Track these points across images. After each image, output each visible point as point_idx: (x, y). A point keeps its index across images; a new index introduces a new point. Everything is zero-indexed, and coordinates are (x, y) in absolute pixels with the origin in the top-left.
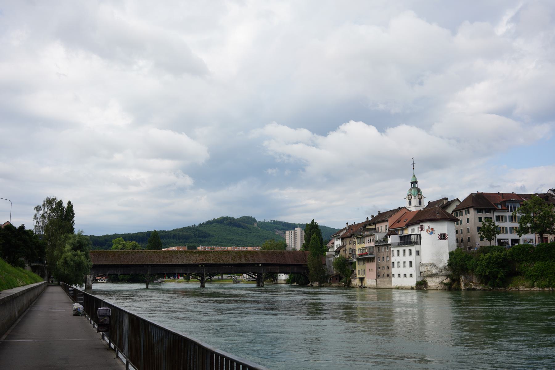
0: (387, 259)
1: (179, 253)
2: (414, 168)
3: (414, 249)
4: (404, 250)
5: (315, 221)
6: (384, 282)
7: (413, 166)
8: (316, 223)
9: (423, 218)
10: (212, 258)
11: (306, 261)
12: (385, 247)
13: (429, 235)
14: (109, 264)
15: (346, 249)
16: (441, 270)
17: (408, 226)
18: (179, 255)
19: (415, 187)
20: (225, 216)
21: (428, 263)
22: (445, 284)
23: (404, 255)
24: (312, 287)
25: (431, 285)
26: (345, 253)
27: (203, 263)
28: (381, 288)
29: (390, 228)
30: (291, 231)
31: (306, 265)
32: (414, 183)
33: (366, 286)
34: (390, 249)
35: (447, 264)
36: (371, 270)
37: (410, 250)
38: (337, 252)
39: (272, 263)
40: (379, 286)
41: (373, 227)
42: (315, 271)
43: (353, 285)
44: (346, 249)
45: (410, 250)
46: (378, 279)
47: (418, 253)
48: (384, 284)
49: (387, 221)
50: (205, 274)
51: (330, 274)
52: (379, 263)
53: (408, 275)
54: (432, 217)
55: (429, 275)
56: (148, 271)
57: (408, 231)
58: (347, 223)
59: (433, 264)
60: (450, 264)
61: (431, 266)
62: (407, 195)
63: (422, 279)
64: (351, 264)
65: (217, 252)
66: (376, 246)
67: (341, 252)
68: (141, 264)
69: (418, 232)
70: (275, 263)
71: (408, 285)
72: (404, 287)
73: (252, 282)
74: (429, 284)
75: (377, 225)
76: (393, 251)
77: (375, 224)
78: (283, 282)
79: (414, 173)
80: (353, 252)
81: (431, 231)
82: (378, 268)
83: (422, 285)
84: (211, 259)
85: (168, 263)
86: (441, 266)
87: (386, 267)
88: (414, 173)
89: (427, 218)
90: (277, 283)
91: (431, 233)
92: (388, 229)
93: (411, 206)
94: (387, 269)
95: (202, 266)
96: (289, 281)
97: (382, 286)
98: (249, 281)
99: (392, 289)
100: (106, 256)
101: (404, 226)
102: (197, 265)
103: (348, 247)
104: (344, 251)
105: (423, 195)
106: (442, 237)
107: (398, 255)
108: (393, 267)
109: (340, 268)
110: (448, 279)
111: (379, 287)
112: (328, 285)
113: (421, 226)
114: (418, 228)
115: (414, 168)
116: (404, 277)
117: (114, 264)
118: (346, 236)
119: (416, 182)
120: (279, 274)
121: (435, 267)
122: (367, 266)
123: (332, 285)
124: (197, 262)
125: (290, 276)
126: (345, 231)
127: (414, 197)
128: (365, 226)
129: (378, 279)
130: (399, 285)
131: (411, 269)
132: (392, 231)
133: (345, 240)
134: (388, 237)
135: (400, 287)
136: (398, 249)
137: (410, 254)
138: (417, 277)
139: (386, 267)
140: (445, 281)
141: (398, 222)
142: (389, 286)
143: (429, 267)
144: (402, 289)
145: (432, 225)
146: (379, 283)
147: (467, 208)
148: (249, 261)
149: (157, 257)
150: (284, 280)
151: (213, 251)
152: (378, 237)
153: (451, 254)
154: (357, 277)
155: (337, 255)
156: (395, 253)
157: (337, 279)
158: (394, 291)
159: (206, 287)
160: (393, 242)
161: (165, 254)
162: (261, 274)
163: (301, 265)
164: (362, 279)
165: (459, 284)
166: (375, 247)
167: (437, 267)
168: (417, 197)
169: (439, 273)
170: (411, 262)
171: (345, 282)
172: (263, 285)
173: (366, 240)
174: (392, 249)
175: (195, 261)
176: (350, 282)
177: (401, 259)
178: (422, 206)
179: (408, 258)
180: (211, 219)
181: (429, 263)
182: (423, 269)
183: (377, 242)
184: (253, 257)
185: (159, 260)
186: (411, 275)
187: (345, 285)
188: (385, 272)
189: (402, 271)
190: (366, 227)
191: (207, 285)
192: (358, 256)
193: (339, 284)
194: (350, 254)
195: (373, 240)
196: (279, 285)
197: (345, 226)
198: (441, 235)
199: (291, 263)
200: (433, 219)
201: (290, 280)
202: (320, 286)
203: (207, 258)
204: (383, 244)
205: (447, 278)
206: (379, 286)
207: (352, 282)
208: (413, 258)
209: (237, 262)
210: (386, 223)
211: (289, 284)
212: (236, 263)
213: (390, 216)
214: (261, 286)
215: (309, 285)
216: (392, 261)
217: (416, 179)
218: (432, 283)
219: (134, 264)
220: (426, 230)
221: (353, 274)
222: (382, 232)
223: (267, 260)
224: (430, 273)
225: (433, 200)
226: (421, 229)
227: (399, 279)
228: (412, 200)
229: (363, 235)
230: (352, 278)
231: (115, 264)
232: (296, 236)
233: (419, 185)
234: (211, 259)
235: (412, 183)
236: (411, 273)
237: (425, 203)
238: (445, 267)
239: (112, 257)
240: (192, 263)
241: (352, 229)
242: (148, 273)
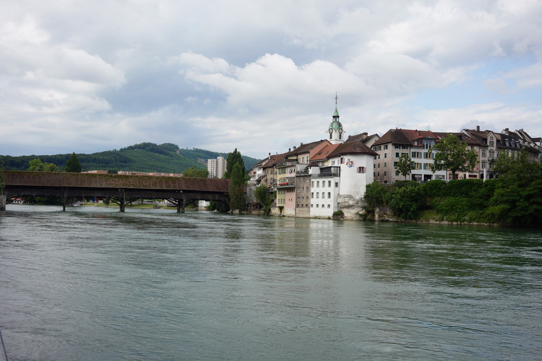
0: (306, 190)
1: (97, 177)
3: (333, 180)
4: (324, 182)
5: (238, 151)
6: (303, 211)
8: (238, 152)
9: (344, 151)
10: (133, 182)
11: (227, 189)
12: (306, 178)
13: (348, 168)
14: (24, 185)
15: (267, 179)
16: (358, 202)
17: (329, 158)
18: (98, 179)
19: (336, 121)
20: (147, 142)
21: (346, 194)
22: (361, 215)
23: (324, 186)
24: (232, 214)
25: (348, 215)
26: (267, 182)
27: (123, 187)
28: (300, 217)
29: (311, 160)
30: (213, 160)
31: (228, 192)
32: (336, 117)
33: (285, 214)
34: (310, 180)
35: (363, 196)
36: (291, 200)
37: (330, 182)
38: (259, 181)
39: (194, 190)
40: (298, 215)
41: (295, 158)
42: (236, 199)
43: (273, 213)
44: (268, 178)
45: (330, 182)
46: (297, 209)
47: (337, 185)
48: (302, 213)
49: (309, 153)
50: (124, 199)
51: (251, 202)
53: (326, 206)
54: (353, 151)
55: (346, 206)
56: (65, 194)
57: (329, 164)
58: (270, 154)
59: (350, 196)
60: (367, 197)
61: (348, 197)
62: (328, 129)
63: (339, 209)
64: (272, 193)
65: (137, 177)
66: (297, 176)
67: (263, 181)
68: (57, 186)
69: (338, 164)
70: (197, 189)
71: (325, 215)
72: (322, 217)
73: (172, 208)
74: (346, 215)
75: (299, 157)
76: (313, 182)
77: (297, 155)
78: (204, 209)
80: (274, 182)
81: (350, 163)
82: (298, 197)
83: (339, 215)
84: (131, 184)
85: (86, 186)
86: (358, 198)
87: (305, 198)
89: (347, 152)
90: (197, 210)
91: (351, 166)
92: (310, 161)
93: (331, 140)
94: (306, 199)
95: (122, 190)
96: (210, 208)
98: (170, 206)
99: (310, 218)
100: (21, 177)
101: (325, 158)
102: (116, 190)
103: (269, 176)
104: (265, 180)
105: (343, 129)
106: (361, 170)
107: (318, 186)
108: (313, 197)
109: (261, 197)
110: (364, 210)
111: (297, 216)
112: (248, 213)
113: (342, 159)
114: (339, 160)
116: (322, 207)
117: (28, 185)
118: (268, 166)
119: (338, 117)
120: (200, 201)
121: (352, 199)
122: (287, 196)
123: (252, 213)
124: (117, 186)
125: (211, 203)
126: (267, 161)
127: (335, 131)
128: (287, 156)
129: (297, 209)
130: (317, 215)
131: (329, 199)
132: (313, 163)
133: (266, 170)
134: (309, 168)
135: (318, 216)
136: (318, 180)
137: (330, 185)
138: (335, 207)
139: (305, 198)
140: (360, 213)
141: (320, 154)
142: (307, 216)
143: (346, 199)
144: (319, 218)
145: (352, 158)
146: (298, 212)
147: (386, 143)
148: (170, 187)
149: (75, 180)
150: (205, 207)
151: (134, 176)
152: (299, 168)
153: (368, 187)
154: (277, 206)
155: (258, 184)
156: (315, 184)
157: (257, 208)
158: (311, 220)
159: (126, 211)
160: (314, 173)
161: (83, 177)
162: (182, 200)
163: (223, 193)
164: (281, 208)
165: (374, 215)
166: (296, 178)
167: (354, 199)
168: (338, 130)
169: (355, 204)
170: (329, 193)
171: (265, 211)
172: (183, 211)
173: (288, 170)
174: (312, 180)
175: (114, 186)
176: (270, 210)
177: (321, 190)
178: (342, 140)
179: (327, 189)
180: (133, 144)
181: (347, 195)
182: (340, 200)
183: (298, 173)
184: (175, 183)
185: (77, 183)
186: (329, 206)
187: (265, 213)
188: (304, 202)
189: (321, 201)
190: (287, 158)
191: (127, 210)
192: (279, 186)
193: (259, 212)
194: (271, 183)
195: (294, 170)
196: (199, 212)
197: (268, 156)
198: (360, 168)
199: (212, 191)
200: (354, 153)
201: (211, 207)
202: (241, 214)
203: (127, 183)
204: (304, 175)
205: (363, 210)
207: (272, 211)
208: (332, 189)
209: (158, 188)
210: (308, 155)
211: (209, 211)
212: (157, 189)
213: (312, 148)
214: (182, 212)
215: (229, 212)
216: (312, 192)
217: (338, 113)
218: (348, 214)
219: (50, 186)
220: (345, 163)
221: (273, 203)
222: (303, 163)
223: (188, 187)
224: (347, 205)
225: (353, 134)
226: (341, 162)
227: (317, 209)
228: (333, 134)
229: (284, 166)
230: (272, 207)
231: (30, 185)
232: (218, 164)
233: (341, 120)
234: (131, 184)
235: (334, 117)
236: (329, 204)
237: (345, 138)
238: (362, 199)
239: (26, 178)
240: (111, 187)
241: (274, 160)
242: (65, 195)
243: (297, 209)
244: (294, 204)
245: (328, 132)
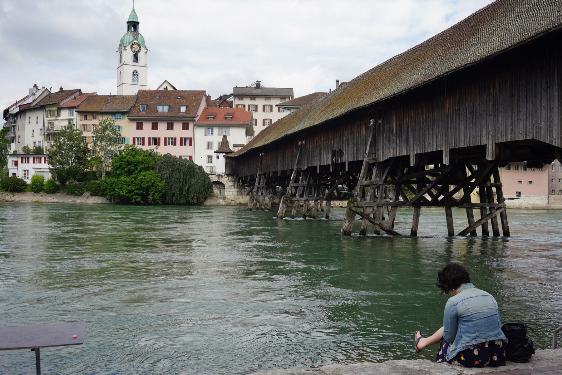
40: (552, 206)
52: (553, 174)
79: (133, 8)
88: (133, 8)
93: (136, 64)
97: (557, 206)
111: (552, 208)
127: (145, 51)
146: (553, 201)
206: (552, 206)
243: (552, 197)
244: (546, 189)
245: (128, 48)
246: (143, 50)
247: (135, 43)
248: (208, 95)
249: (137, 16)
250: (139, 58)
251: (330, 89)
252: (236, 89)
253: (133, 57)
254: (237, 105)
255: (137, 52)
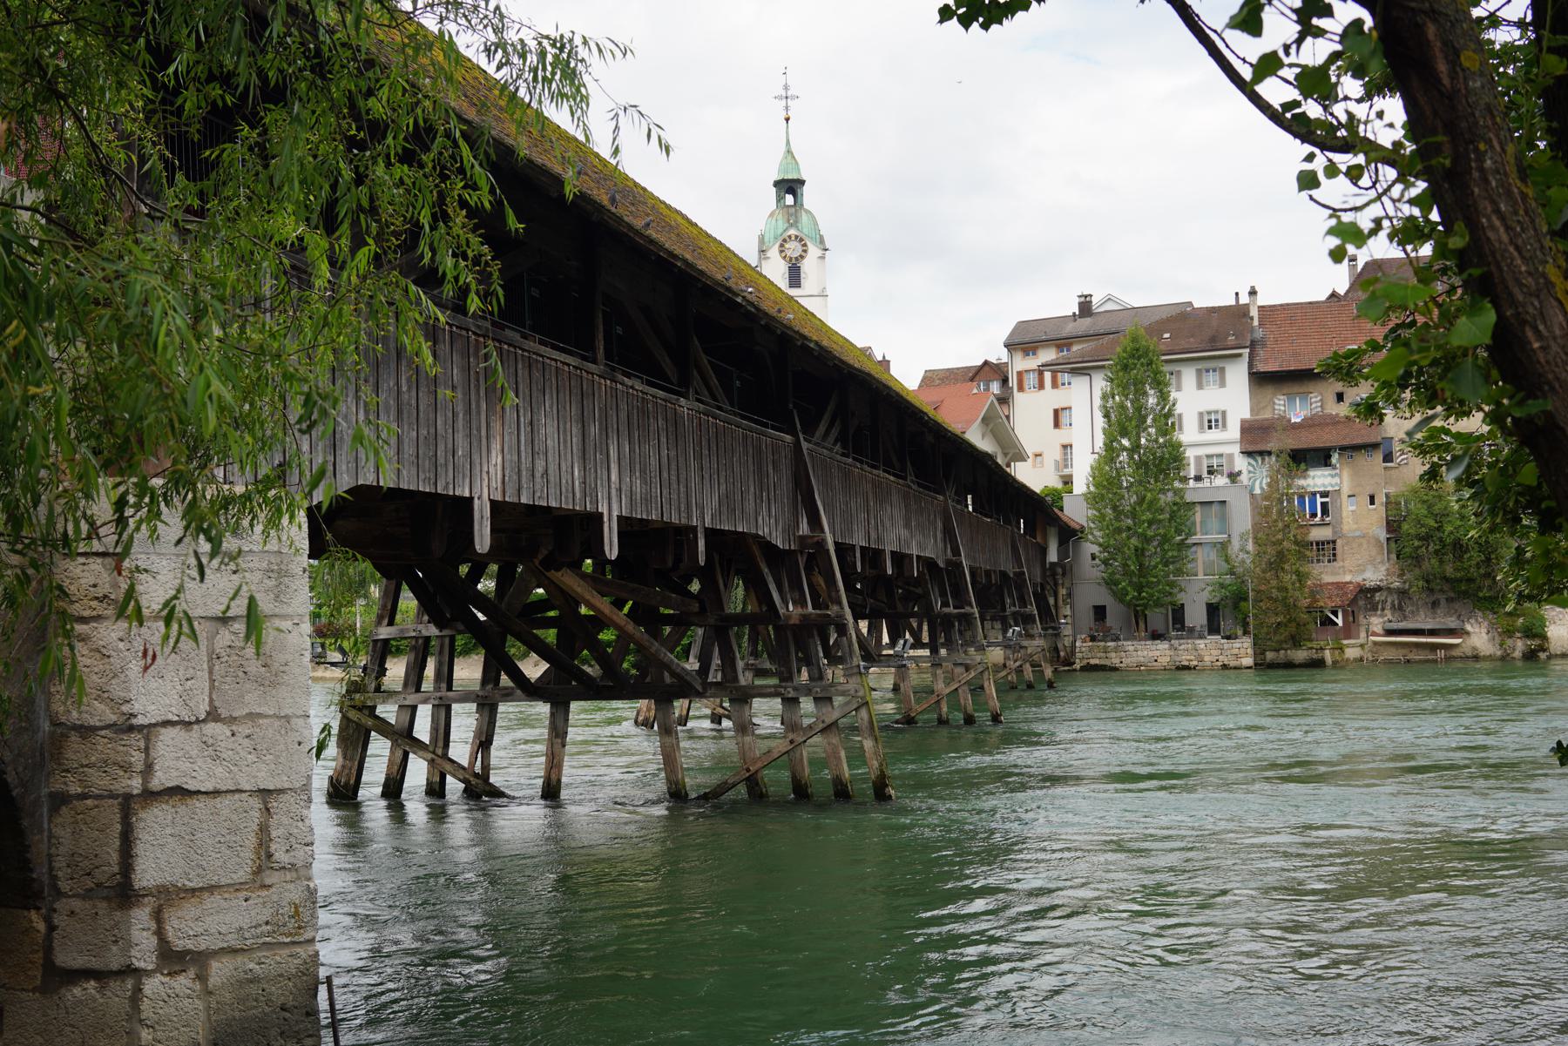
2: (787, 120)
7: (787, 108)
32: (790, 187)
58: (1253, 293)
79: (788, 142)
88: (788, 142)
115: (787, 120)
127: (820, 253)
246: (814, 251)
247: (790, 237)
248: (880, 358)
249: (797, 163)
250: (802, 275)
251: (1237, 294)
252: (1022, 326)
253: (787, 275)
254: (1020, 374)
255: (796, 259)
